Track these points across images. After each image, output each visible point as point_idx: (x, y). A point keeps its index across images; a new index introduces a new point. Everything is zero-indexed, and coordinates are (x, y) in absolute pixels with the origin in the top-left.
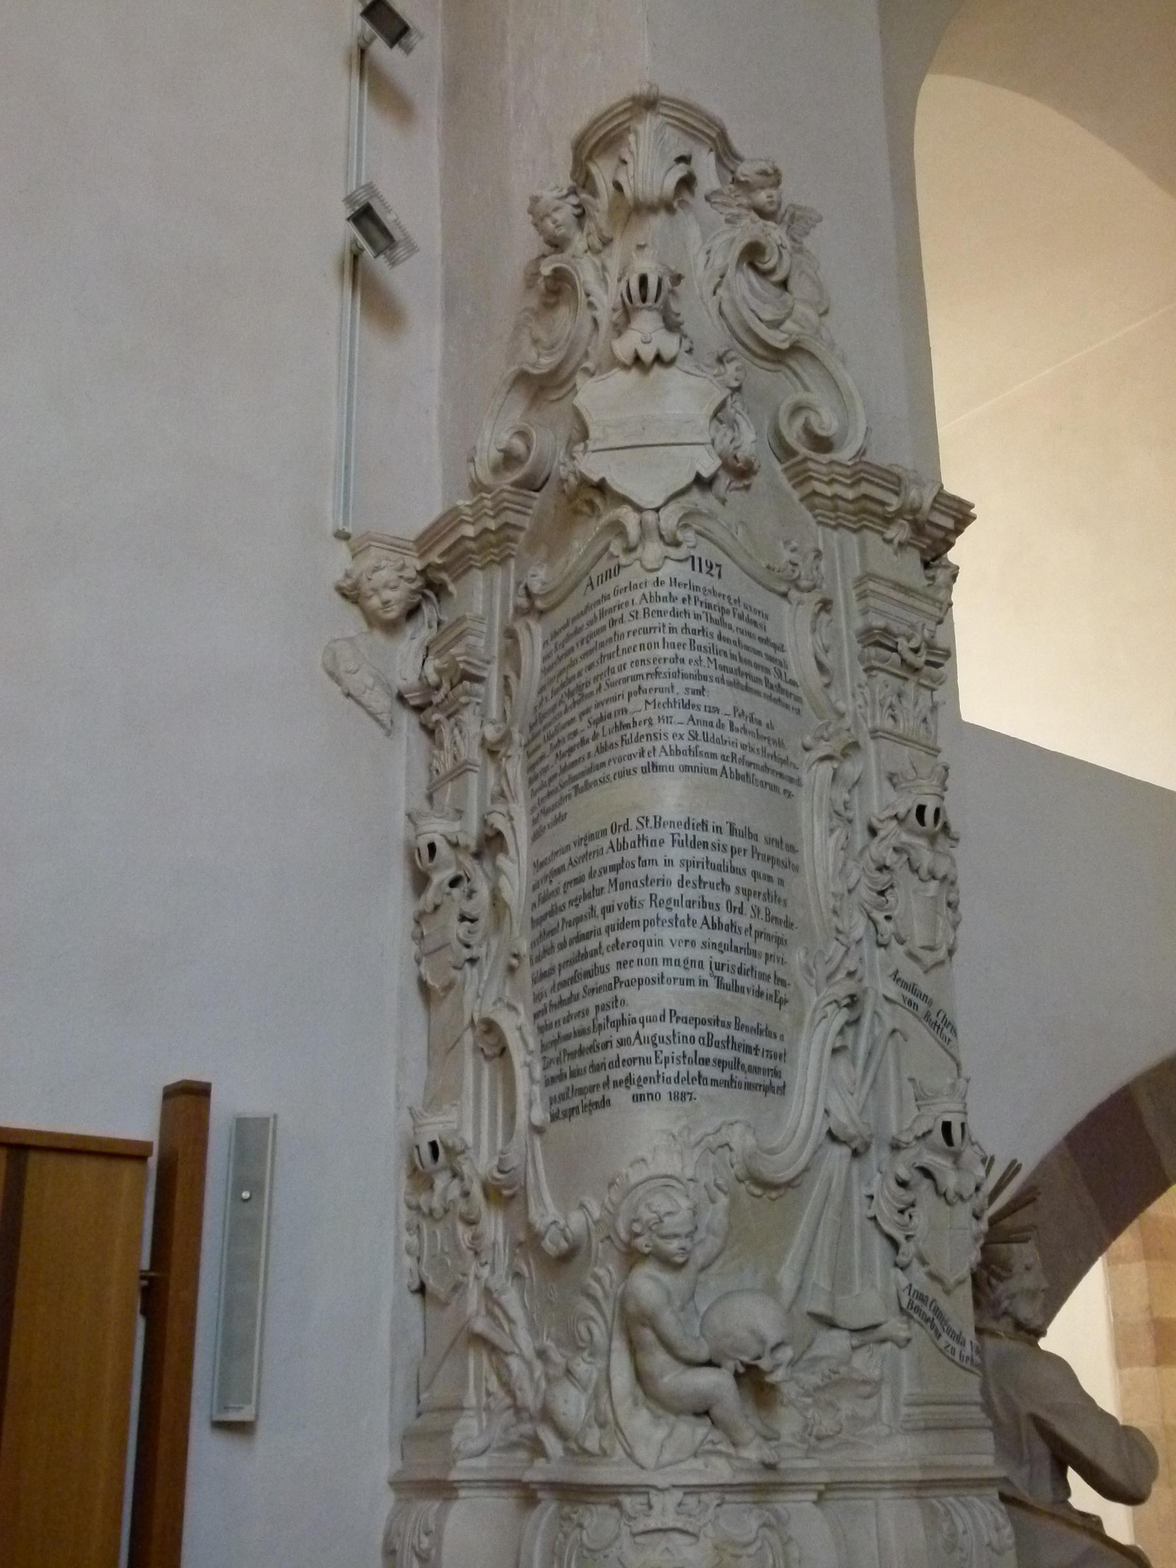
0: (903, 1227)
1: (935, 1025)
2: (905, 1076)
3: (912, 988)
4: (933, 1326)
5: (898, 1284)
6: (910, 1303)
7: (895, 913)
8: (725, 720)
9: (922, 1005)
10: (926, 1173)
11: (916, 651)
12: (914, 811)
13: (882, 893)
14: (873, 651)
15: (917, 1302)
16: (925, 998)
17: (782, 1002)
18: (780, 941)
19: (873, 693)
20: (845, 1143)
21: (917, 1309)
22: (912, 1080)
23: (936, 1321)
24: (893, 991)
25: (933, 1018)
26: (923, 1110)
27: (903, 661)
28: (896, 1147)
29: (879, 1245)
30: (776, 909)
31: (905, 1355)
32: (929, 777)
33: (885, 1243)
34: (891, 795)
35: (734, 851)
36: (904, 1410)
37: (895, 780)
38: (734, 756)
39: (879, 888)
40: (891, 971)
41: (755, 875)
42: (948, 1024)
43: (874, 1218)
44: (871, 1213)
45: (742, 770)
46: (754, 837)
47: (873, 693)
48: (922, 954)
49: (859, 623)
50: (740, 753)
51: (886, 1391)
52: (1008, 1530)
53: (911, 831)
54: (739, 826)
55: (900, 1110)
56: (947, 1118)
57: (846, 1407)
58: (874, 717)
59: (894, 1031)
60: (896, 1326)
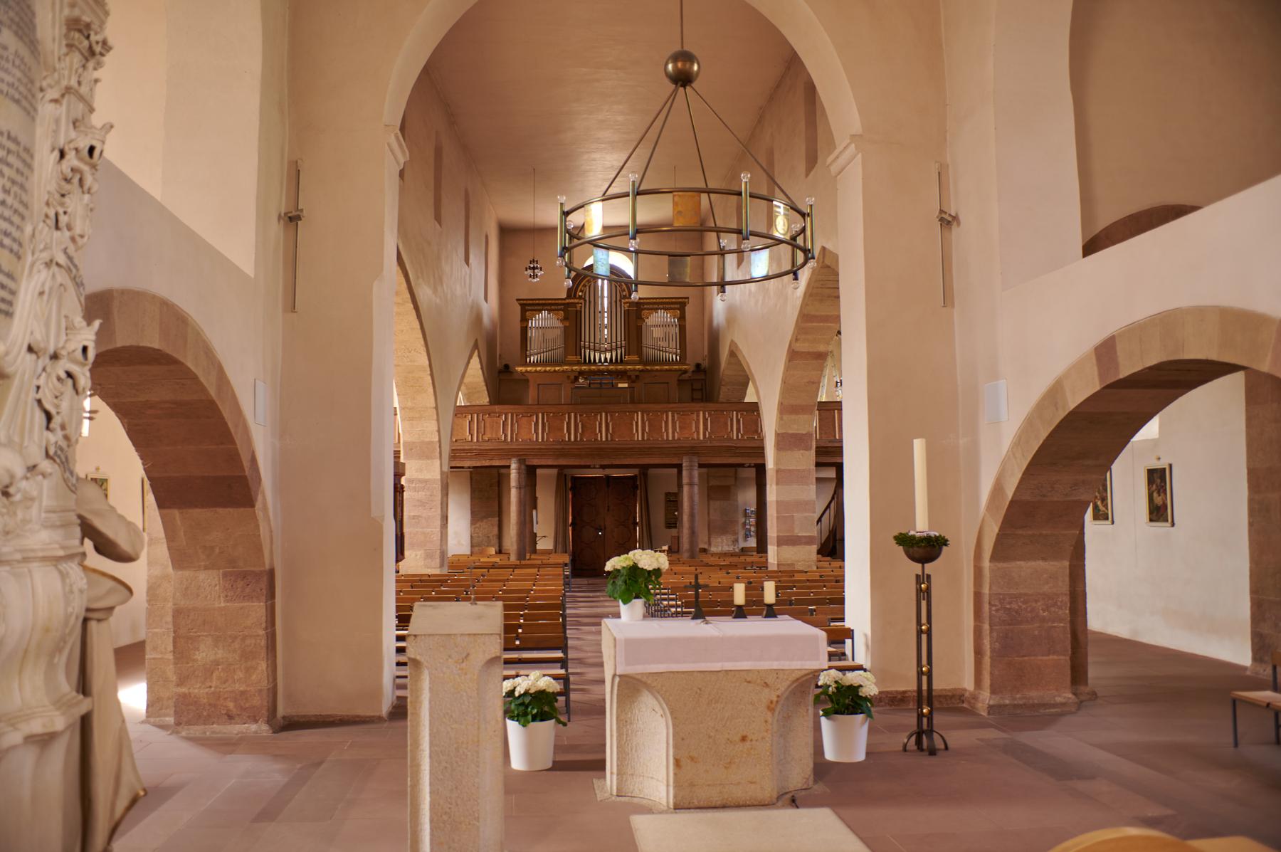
0: (57, 406)
1: (77, 284)
2: (64, 313)
3: (70, 258)
4: (64, 467)
5: (48, 441)
6: (56, 452)
7: (69, 210)
8: (11, 57)
9: (74, 271)
10: (69, 375)
11: (97, 43)
12: (87, 148)
13: (63, 196)
14: (77, 35)
15: (59, 452)
16: (75, 266)
17: (19, 258)
18: (23, 218)
19: (71, 63)
20: (36, 353)
21: (59, 457)
22: (66, 317)
23: (66, 464)
24: (62, 259)
25: (77, 279)
26: (70, 337)
27: (90, 47)
28: (55, 357)
29: (40, 417)
30: (25, 198)
31: (46, 483)
32: (101, 129)
33: (43, 417)
34: (73, 134)
35: (9, 152)
36: (43, 515)
37: (77, 124)
38: (13, 85)
39: (63, 192)
40: (63, 247)
41: (18, 171)
42: (82, 284)
43: (39, 402)
44: (38, 397)
45: (17, 96)
46: (18, 143)
47: (71, 63)
48: (78, 239)
49: (66, 12)
50: (16, 84)
51: (36, 505)
52: (85, 581)
53: (81, 159)
54: (13, 134)
55: (58, 335)
56: (86, 343)
57: (20, 515)
58: (70, 78)
59: (61, 285)
60: (46, 465)
